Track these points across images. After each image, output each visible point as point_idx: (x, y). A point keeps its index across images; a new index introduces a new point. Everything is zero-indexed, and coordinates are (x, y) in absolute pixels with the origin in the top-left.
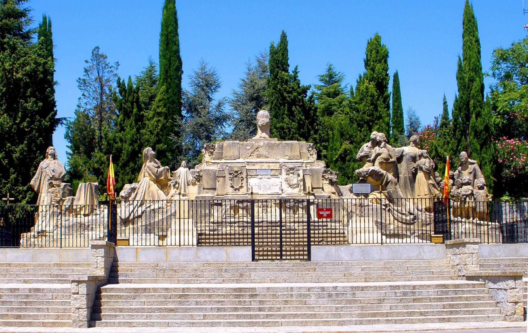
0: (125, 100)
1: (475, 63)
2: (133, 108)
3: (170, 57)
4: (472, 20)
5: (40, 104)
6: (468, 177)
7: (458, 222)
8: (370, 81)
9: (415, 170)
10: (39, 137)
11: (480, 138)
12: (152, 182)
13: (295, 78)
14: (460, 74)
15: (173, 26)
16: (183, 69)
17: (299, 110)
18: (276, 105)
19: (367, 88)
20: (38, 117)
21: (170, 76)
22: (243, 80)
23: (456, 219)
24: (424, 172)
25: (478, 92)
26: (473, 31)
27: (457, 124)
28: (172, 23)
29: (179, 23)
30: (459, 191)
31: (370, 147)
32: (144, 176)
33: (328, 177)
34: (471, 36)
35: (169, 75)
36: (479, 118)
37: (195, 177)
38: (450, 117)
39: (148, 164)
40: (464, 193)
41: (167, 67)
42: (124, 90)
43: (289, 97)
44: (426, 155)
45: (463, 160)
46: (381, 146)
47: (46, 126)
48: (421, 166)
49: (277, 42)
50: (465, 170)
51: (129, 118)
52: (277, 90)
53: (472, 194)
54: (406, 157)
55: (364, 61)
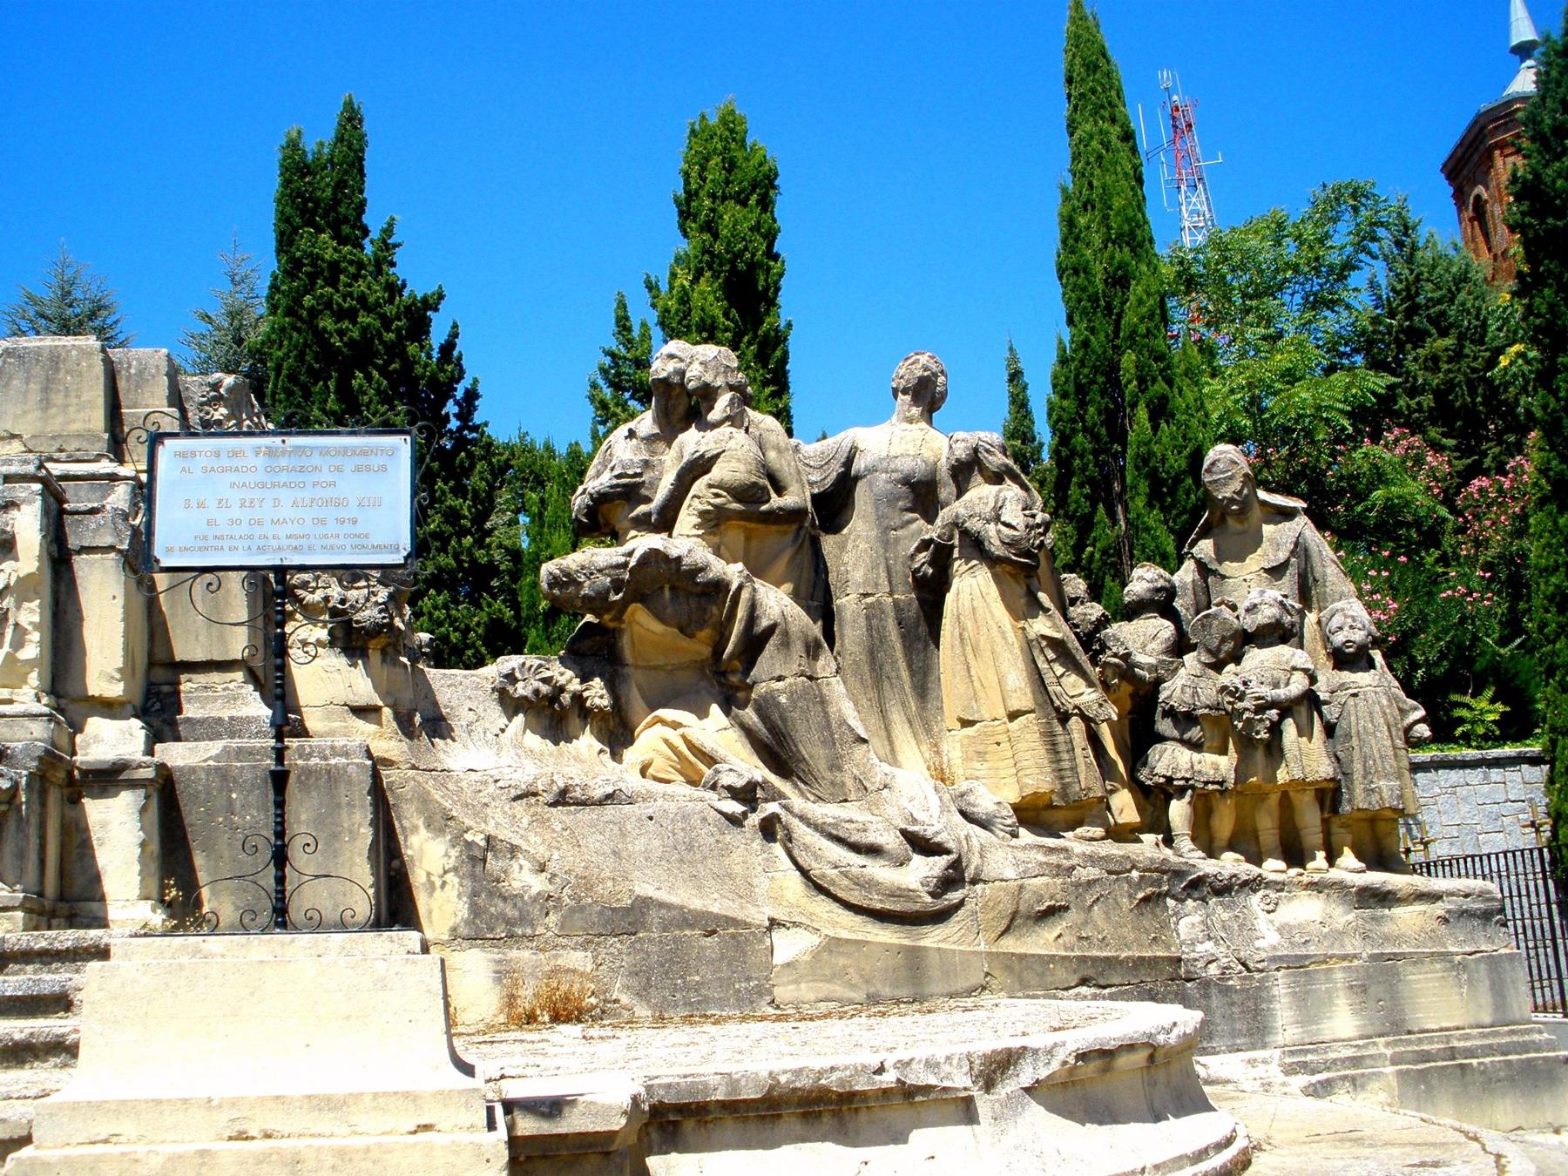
1: (1130, 213)
4: (1102, 62)
6: (1274, 594)
7: (1224, 889)
8: (698, 274)
9: (931, 563)
11: (1173, 506)
13: (382, 261)
14: (1072, 252)
17: (379, 384)
18: (292, 378)
19: (684, 299)
22: (206, 318)
23: (1208, 867)
24: (991, 561)
25: (1151, 317)
26: (1110, 104)
27: (1073, 453)
30: (1230, 676)
31: (650, 440)
33: (327, 599)
34: (1103, 118)
36: (1163, 425)
38: (1043, 431)
40: (1268, 692)
43: (341, 333)
44: (997, 460)
45: (1226, 493)
46: (713, 416)
48: (974, 525)
49: (319, 137)
50: (1241, 558)
52: (300, 318)
53: (1310, 700)
54: (870, 484)
55: (677, 200)
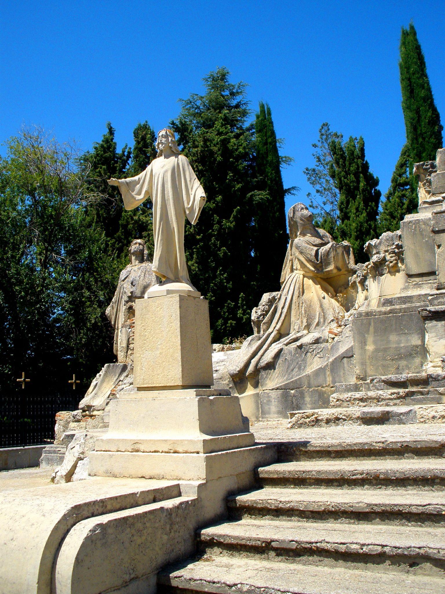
0: (345, 172)
2: (358, 182)
3: (419, 108)
5: (219, 198)
10: (221, 246)
12: (311, 282)
15: (416, 63)
16: (442, 123)
20: (216, 218)
21: (421, 134)
28: (415, 60)
29: (426, 60)
32: (292, 270)
35: (419, 132)
37: (394, 252)
39: (300, 240)
41: (415, 122)
42: (343, 157)
47: (230, 228)
51: (354, 198)
